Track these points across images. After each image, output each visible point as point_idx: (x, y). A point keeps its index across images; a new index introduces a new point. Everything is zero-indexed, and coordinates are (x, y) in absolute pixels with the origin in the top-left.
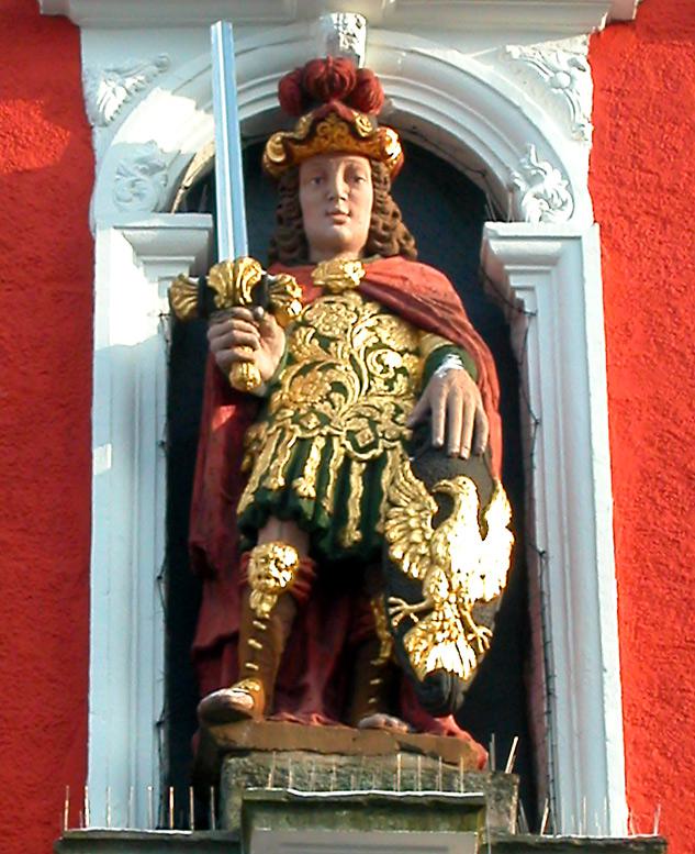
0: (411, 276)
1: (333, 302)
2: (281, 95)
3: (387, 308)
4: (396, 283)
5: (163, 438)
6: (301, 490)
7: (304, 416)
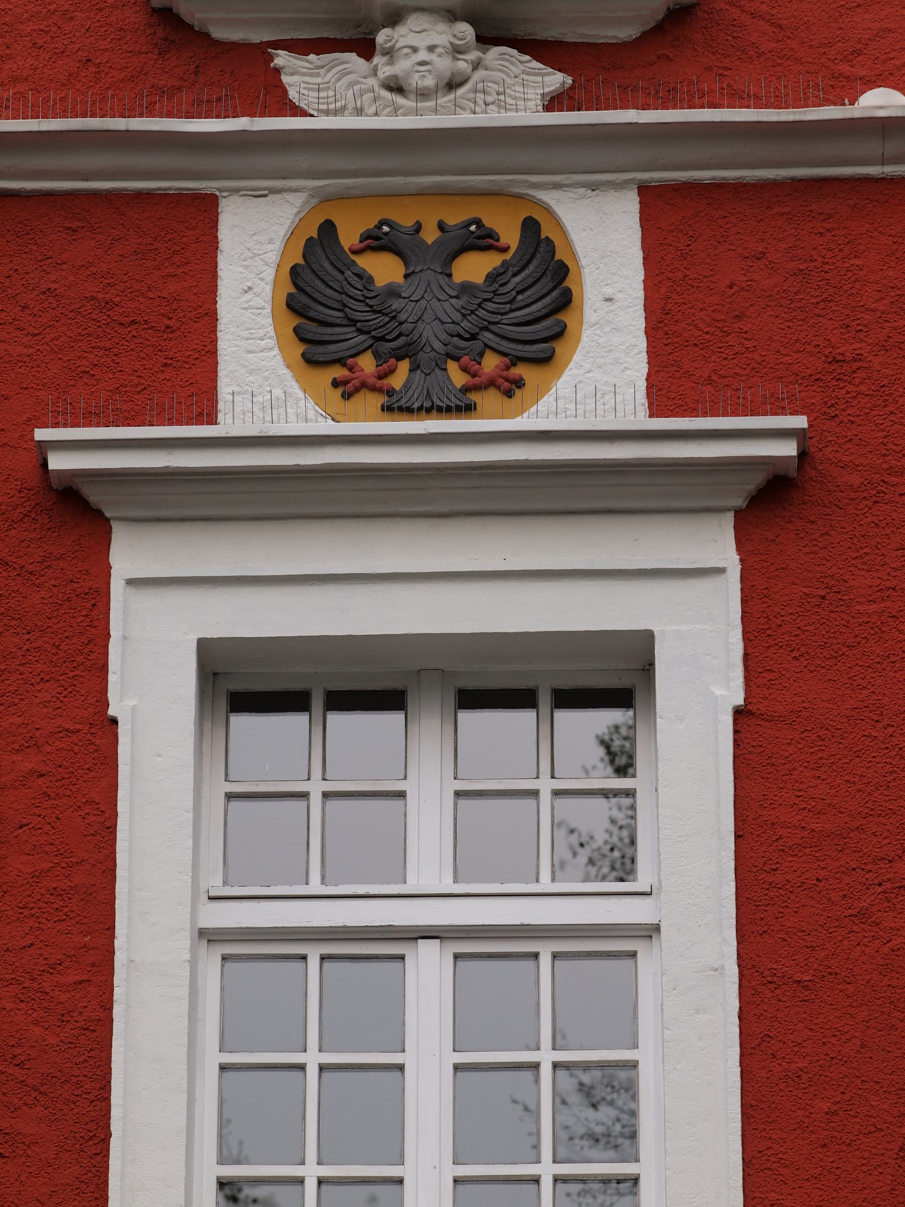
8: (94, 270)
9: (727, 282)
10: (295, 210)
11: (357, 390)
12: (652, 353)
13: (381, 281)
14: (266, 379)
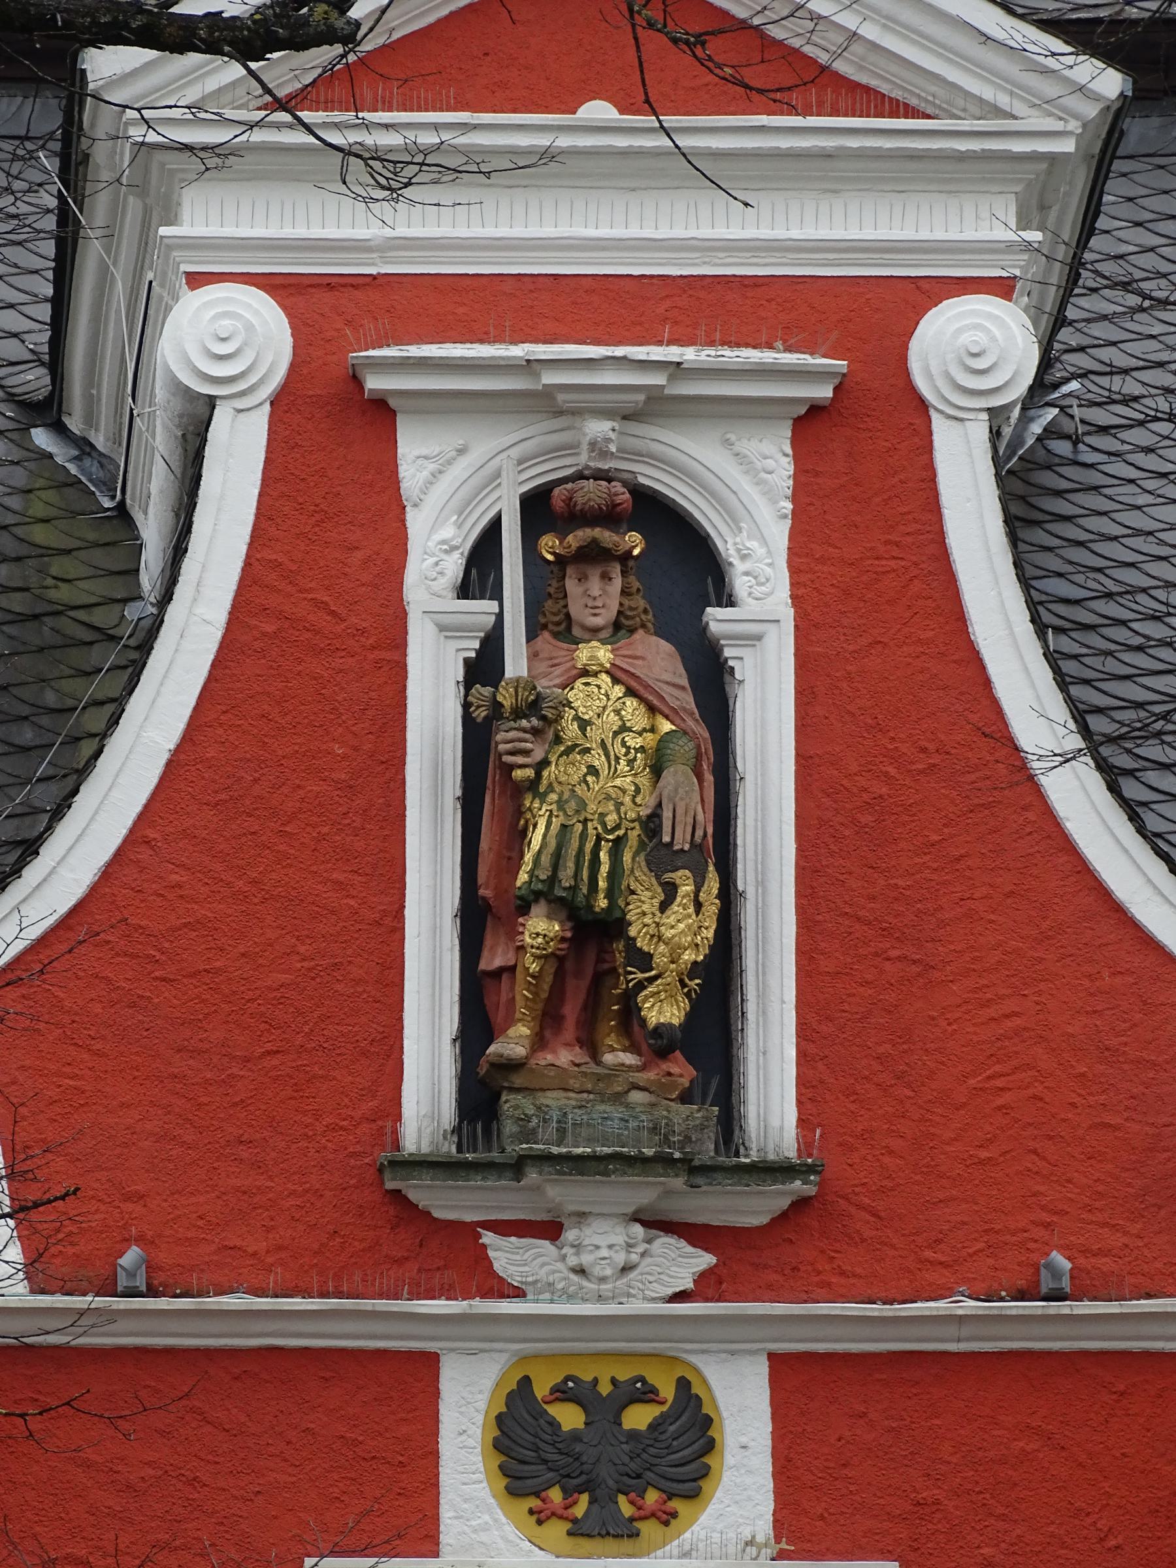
5: (459, 793)
8: (343, 1412)
9: (837, 1436)
11: (548, 1518)
12: (778, 1494)
13: (566, 1427)
14: (477, 1507)
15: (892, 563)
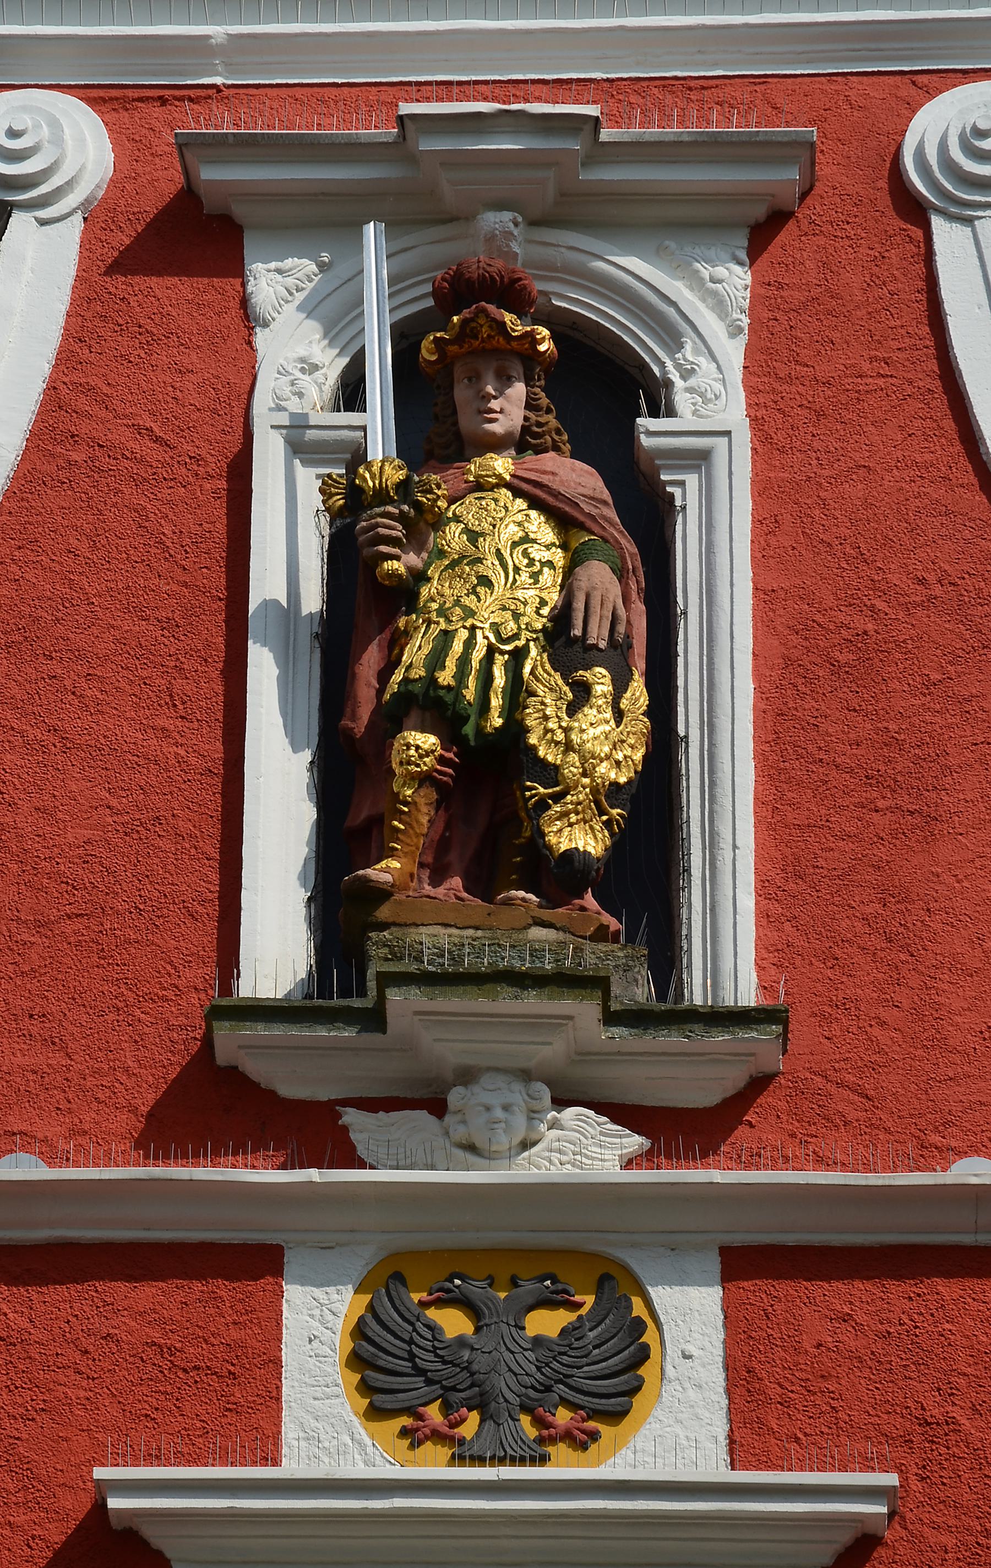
0: (561, 472)
1: (484, 498)
2: (436, 293)
3: (534, 503)
4: (545, 479)
6: (440, 680)
7: (449, 608)
10: (364, 1262)
15: (881, 382)
